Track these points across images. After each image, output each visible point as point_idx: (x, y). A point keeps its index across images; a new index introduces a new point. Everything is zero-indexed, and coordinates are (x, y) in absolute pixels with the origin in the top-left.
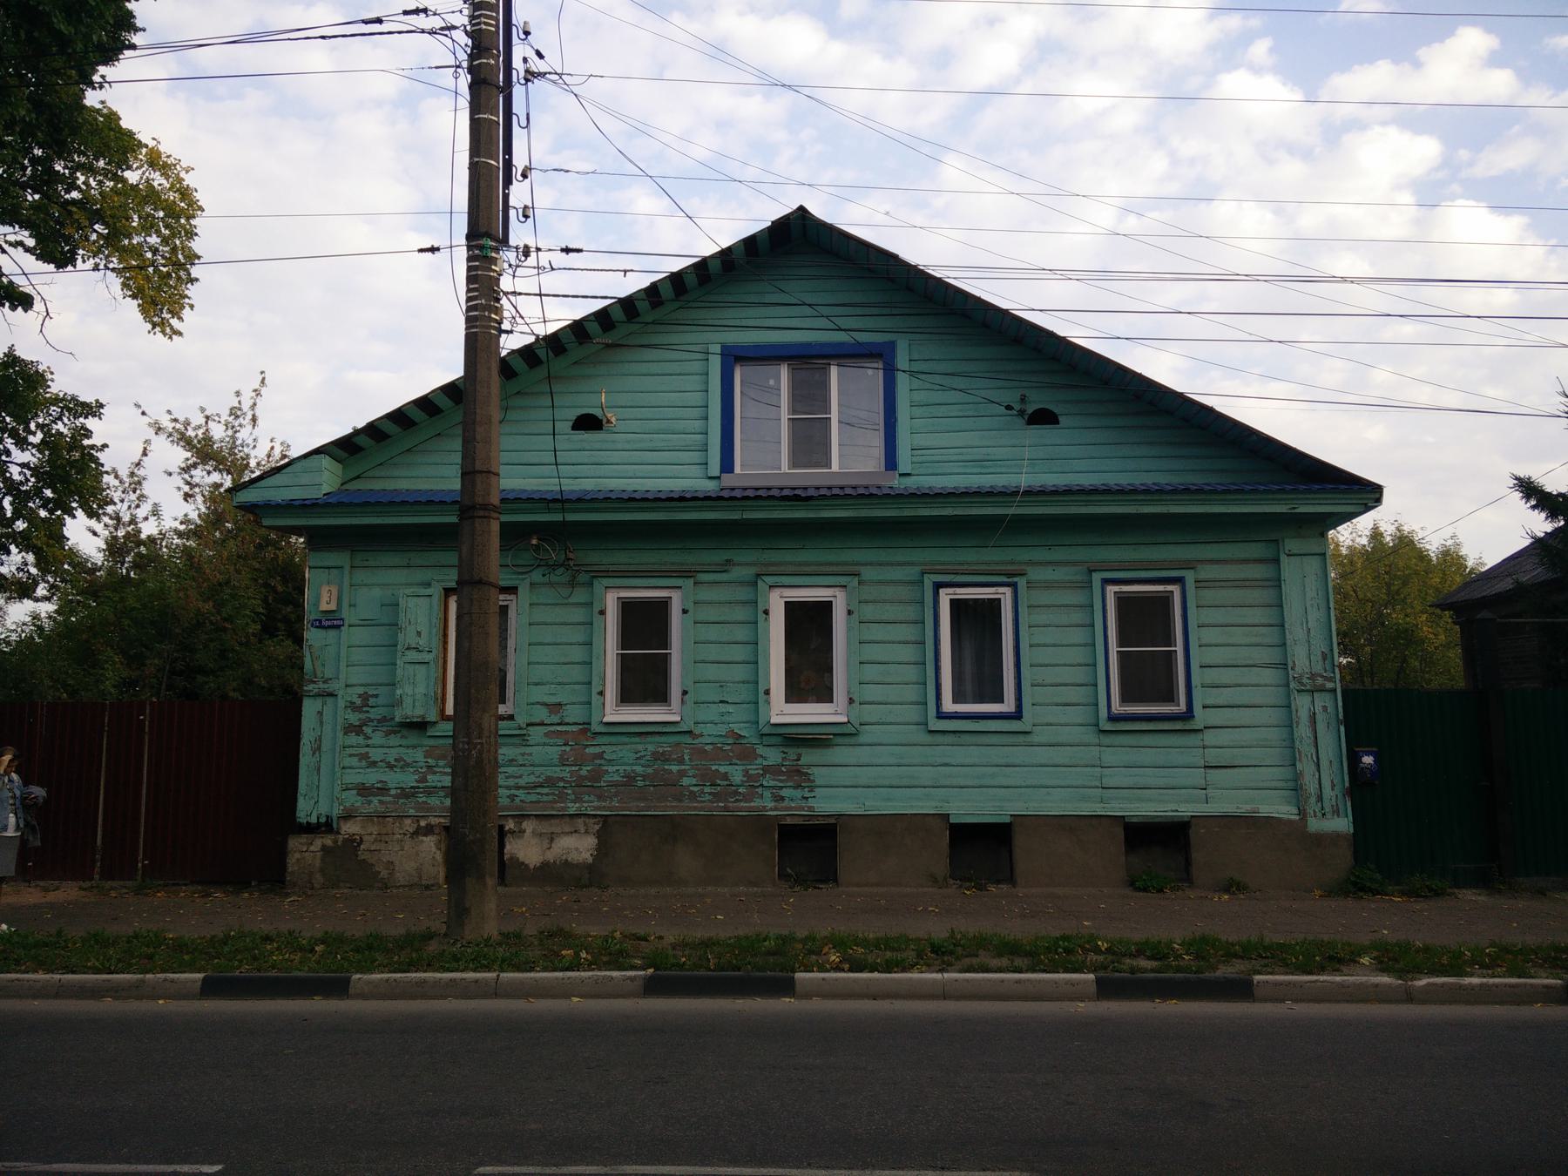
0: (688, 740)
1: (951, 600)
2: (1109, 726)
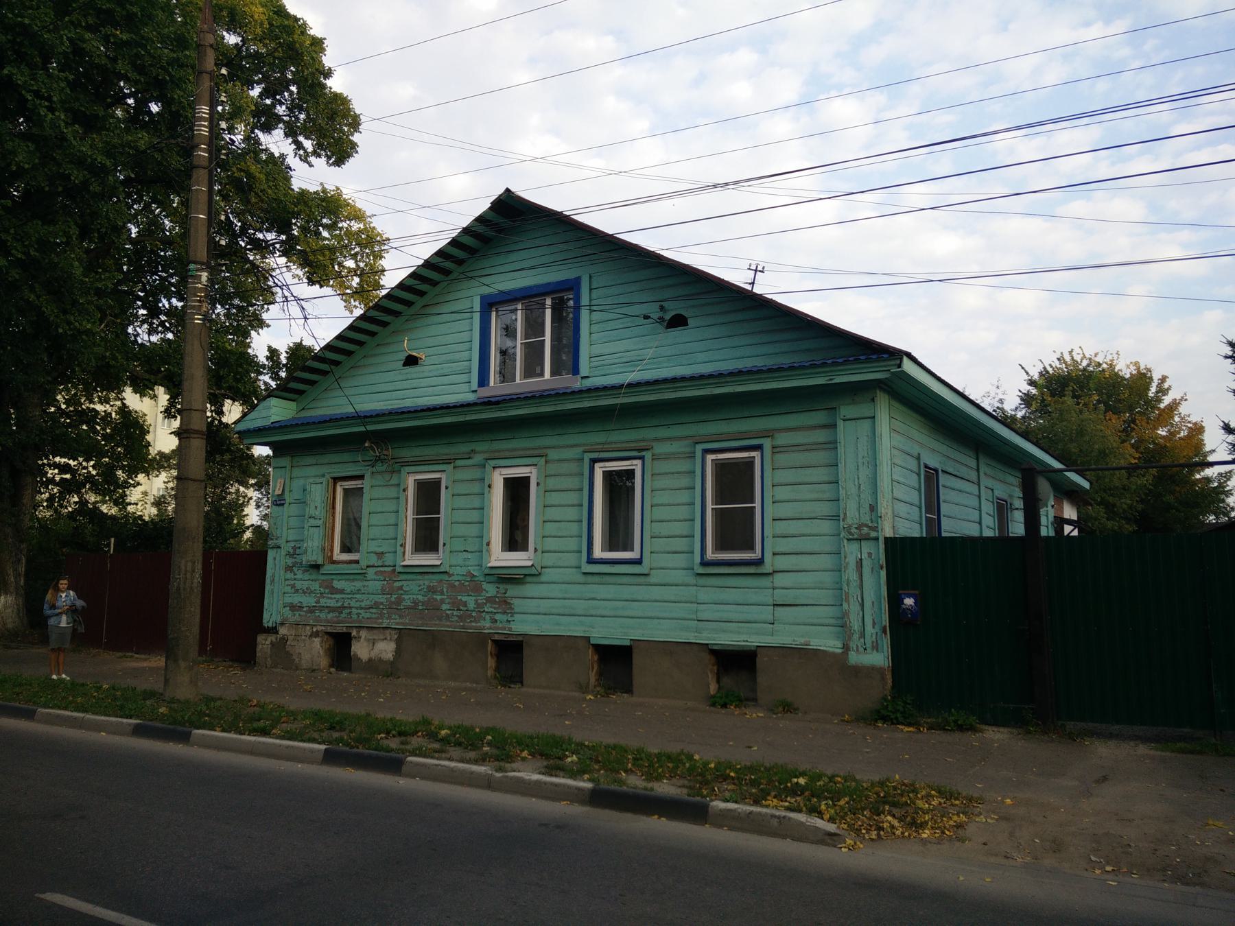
0: (445, 577)
1: (603, 471)
2: (701, 570)
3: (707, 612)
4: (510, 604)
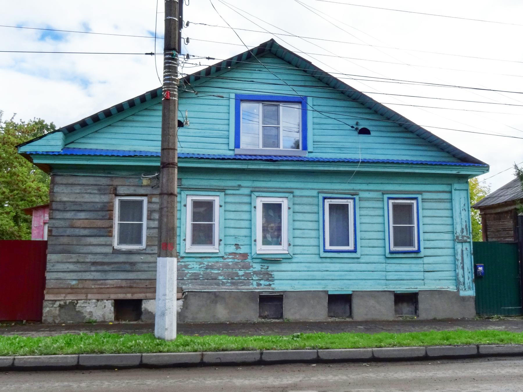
0: (221, 260)
1: (329, 204)
2: (389, 256)
3: (391, 276)
4: (271, 275)
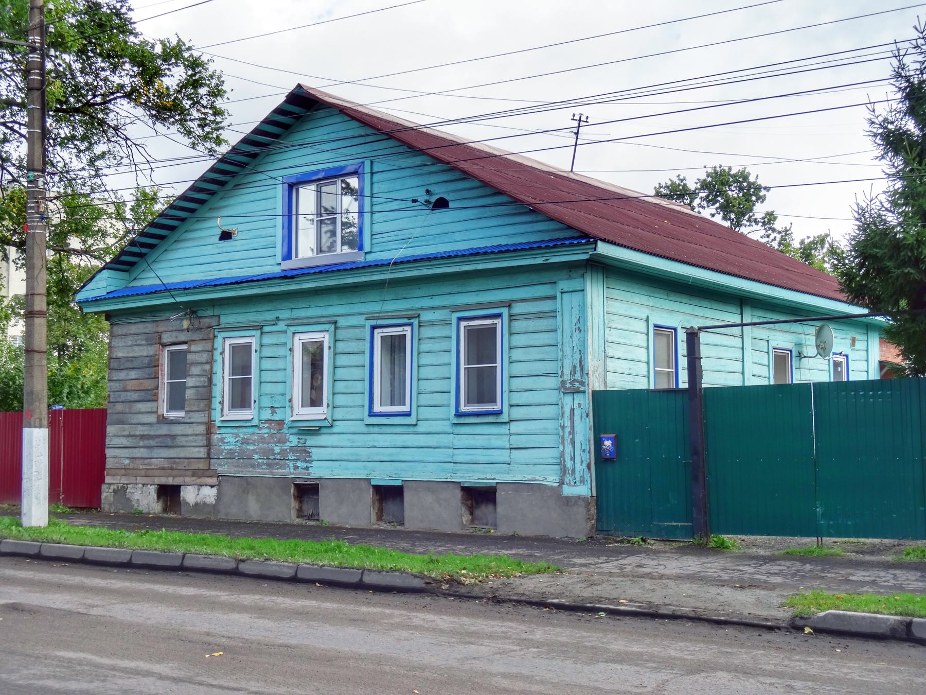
0: (256, 430)
3: (461, 456)
4: (309, 453)
